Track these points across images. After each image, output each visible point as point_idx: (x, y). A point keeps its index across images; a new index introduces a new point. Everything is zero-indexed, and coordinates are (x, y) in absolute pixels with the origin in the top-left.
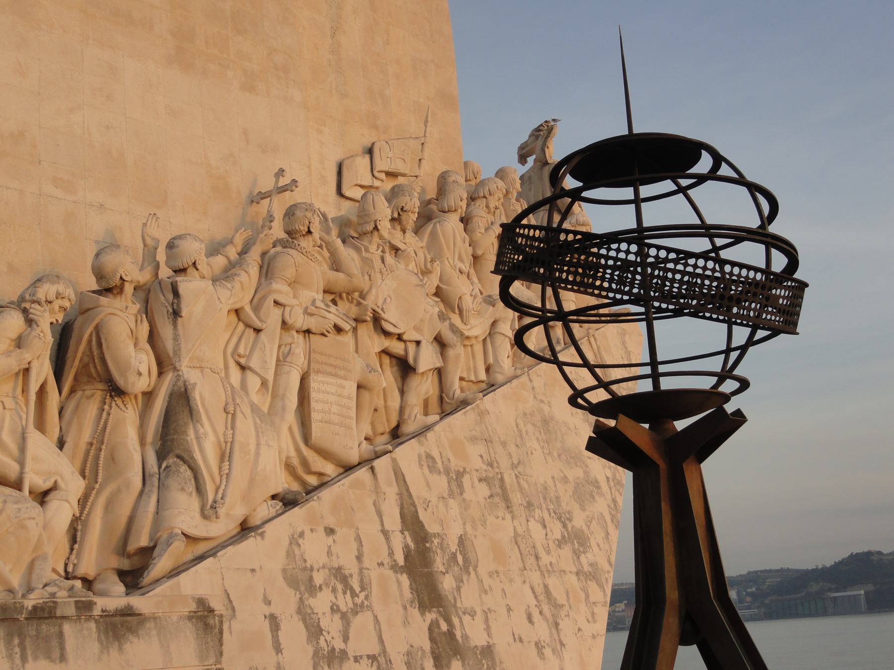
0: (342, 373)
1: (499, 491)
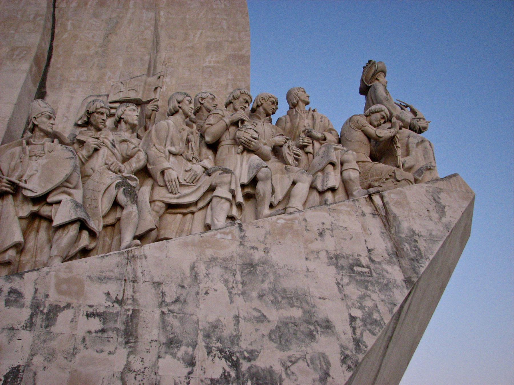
1: (120, 325)
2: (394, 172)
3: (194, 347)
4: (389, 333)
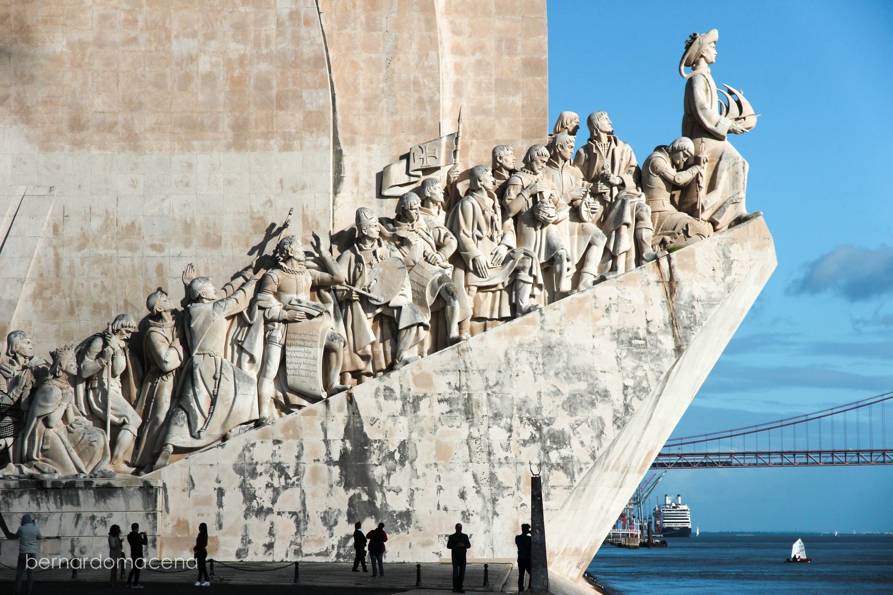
0: (310, 344)
1: (461, 407)
2: (687, 226)
3: (511, 418)
4: (657, 393)
